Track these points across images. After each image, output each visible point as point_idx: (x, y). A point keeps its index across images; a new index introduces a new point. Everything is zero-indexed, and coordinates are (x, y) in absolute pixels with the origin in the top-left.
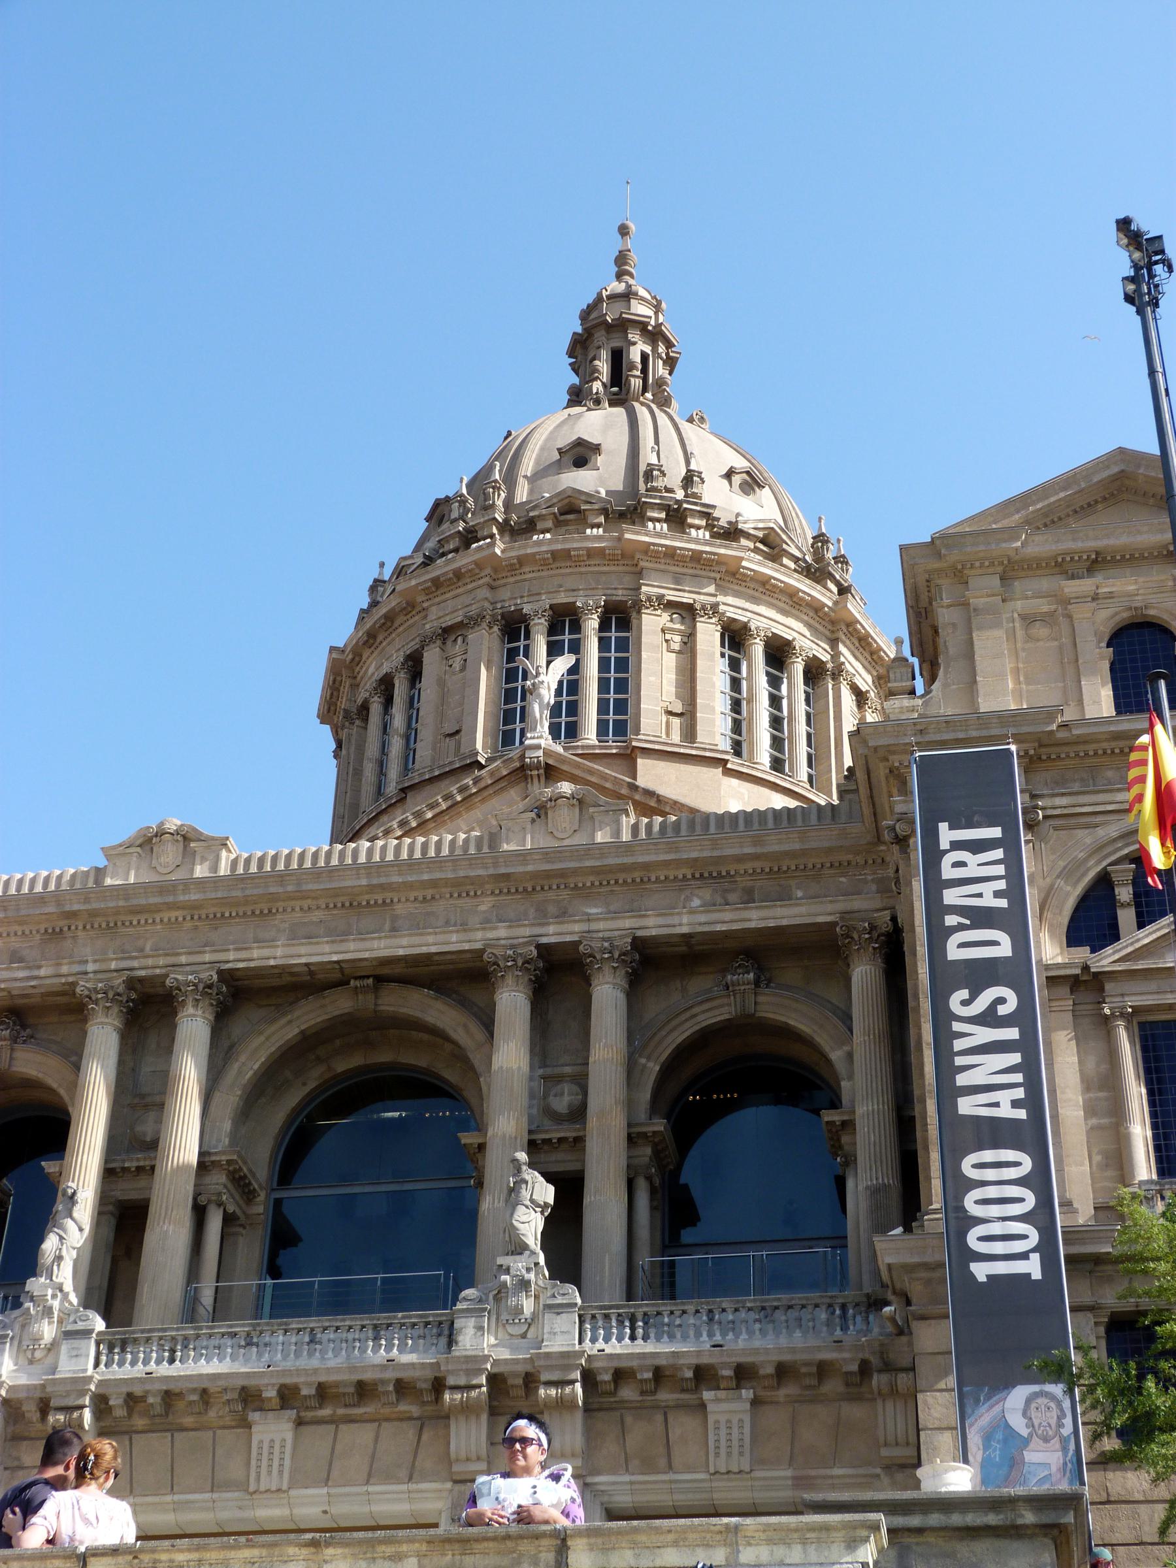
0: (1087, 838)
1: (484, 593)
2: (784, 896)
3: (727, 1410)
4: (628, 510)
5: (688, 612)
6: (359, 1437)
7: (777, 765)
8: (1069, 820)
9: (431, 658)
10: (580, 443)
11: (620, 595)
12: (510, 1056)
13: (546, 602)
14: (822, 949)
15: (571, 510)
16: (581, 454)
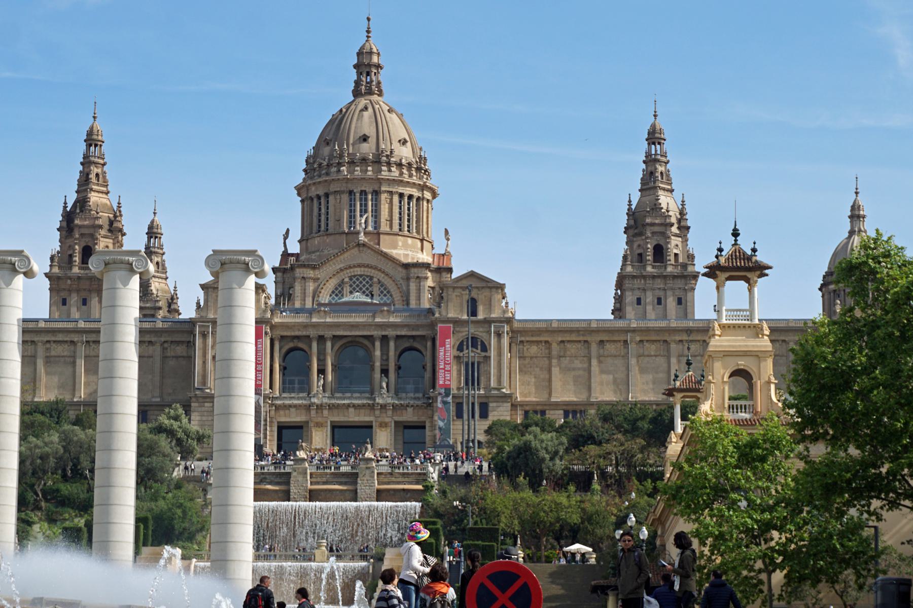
0: (461, 335)
1: (344, 185)
2: (418, 330)
3: (410, 410)
4: (377, 162)
5: (391, 193)
6: (362, 411)
7: (409, 227)
8: (459, 332)
9: (331, 198)
10: (365, 135)
11: (376, 189)
12: (378, 353)
13: (359, 189)
14: (423, 337)
15: (364, 160)
16: (365, 139)
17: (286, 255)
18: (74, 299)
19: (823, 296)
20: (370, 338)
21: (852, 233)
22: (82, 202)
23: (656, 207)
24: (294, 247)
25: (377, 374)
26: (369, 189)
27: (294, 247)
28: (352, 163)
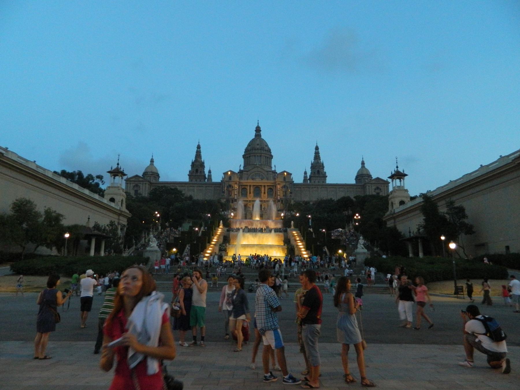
12: (263, 189)
14: (273, 186)
15: (258, 149)
16: (258, 145)
17: (240, 170)
18: (194, 180)
19: (356, 181)
20: (261, 186)
21: (362, 167)
22: (196, 160)
23: (318, 162)
24: (242, 169)
25: (263, 194)
26: (259, 155)
27: (242, 169)
28: (255, 150)
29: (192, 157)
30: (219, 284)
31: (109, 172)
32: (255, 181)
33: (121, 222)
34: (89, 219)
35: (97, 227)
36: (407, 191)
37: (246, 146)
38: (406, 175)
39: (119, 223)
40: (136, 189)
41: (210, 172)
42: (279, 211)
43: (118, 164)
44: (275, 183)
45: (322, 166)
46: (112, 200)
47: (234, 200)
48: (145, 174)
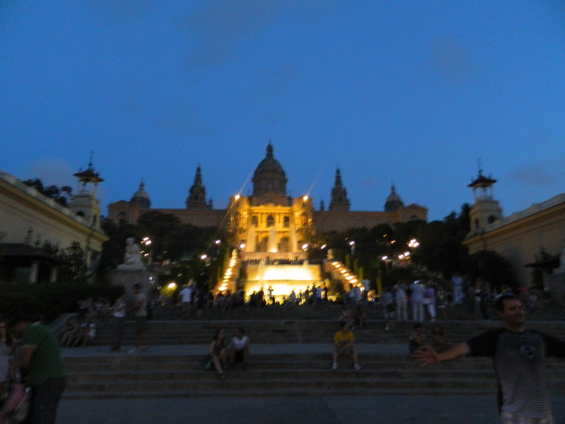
14: (289, 213)
20: (275, 213)
29: (191, 183)
30: (362, 357)
31: (77, 175)
32: (266, 208)
33: (91, 246)
34: (30, 232)
35: (49, 249)
36: (496, 202)
37: (255, 167)
38: (494, 181)
39: (88, 248)
40: (122, 217)
41: (211, 201)
42: (300, 243)
43: (90, 165)
44: (291, 210)
45: (344, 192)
46: (80, 214)
47: (242, 231)
48: (134, 200)
